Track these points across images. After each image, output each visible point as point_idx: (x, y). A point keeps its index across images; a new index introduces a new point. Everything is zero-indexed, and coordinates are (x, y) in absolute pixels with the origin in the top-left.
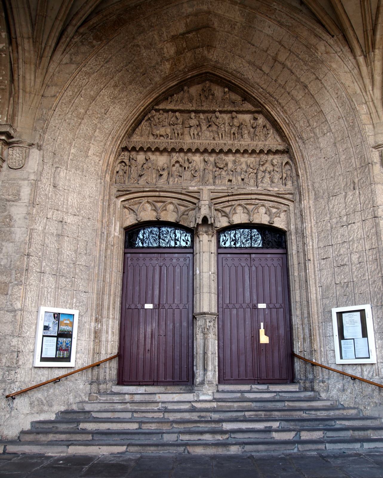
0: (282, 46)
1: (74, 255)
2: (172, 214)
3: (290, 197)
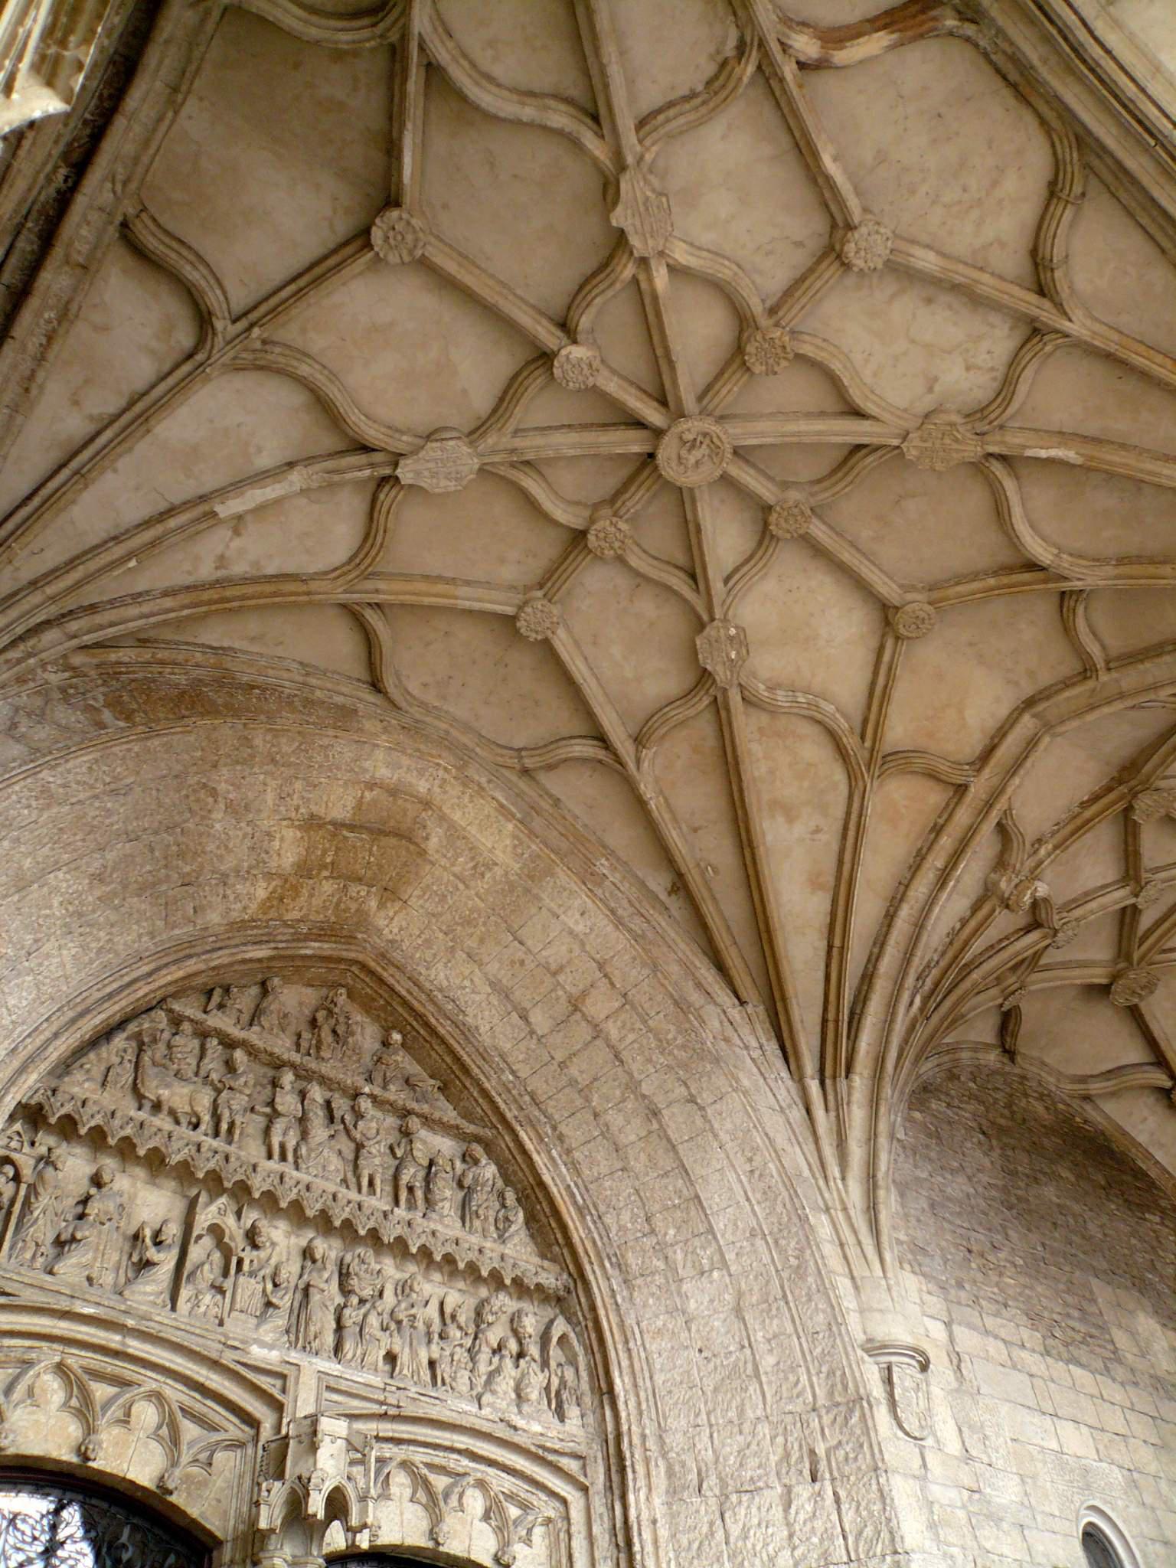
0: (606, 976)
2: (146, 1445)
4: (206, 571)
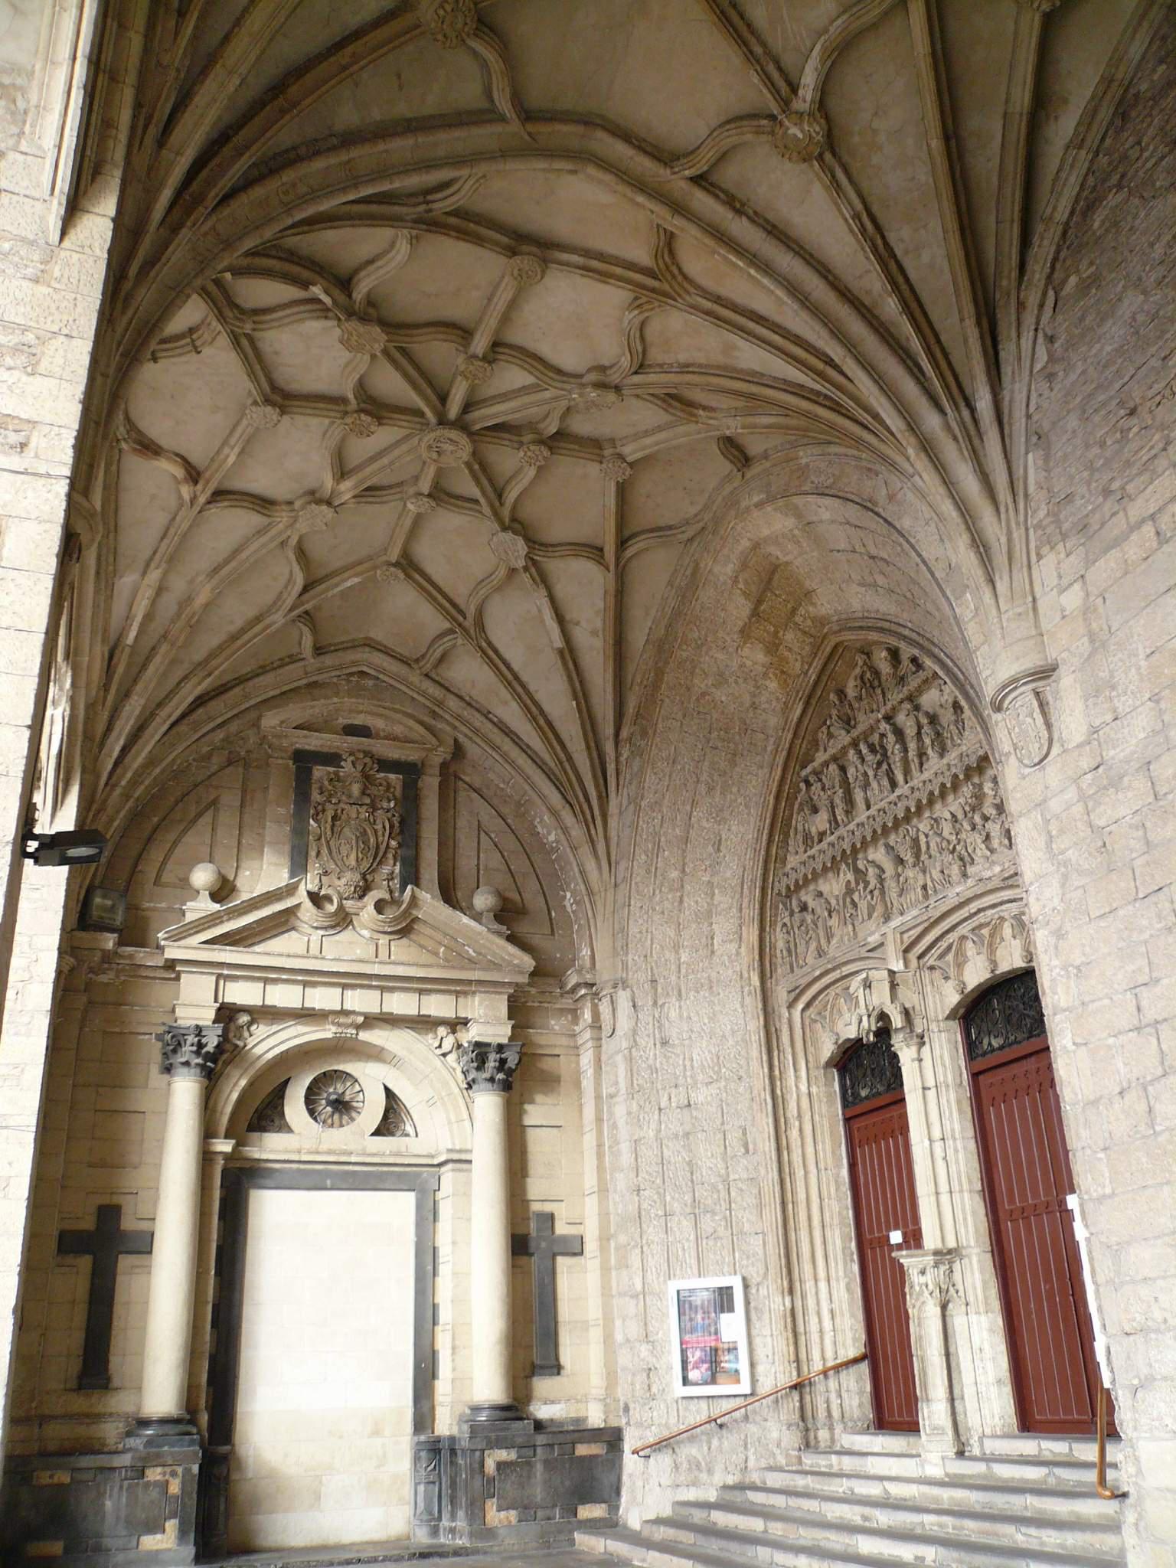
1: (721, 1165)
4: (598, 643)
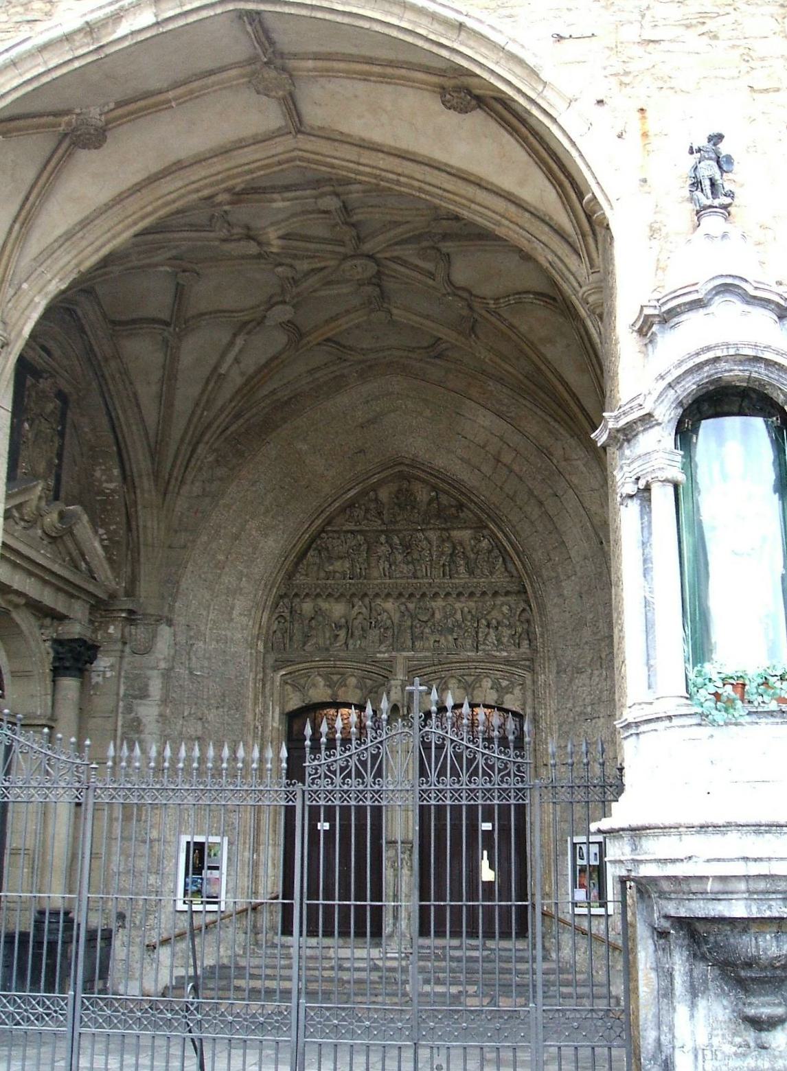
3: (527, 663)
4: (239, 381)
